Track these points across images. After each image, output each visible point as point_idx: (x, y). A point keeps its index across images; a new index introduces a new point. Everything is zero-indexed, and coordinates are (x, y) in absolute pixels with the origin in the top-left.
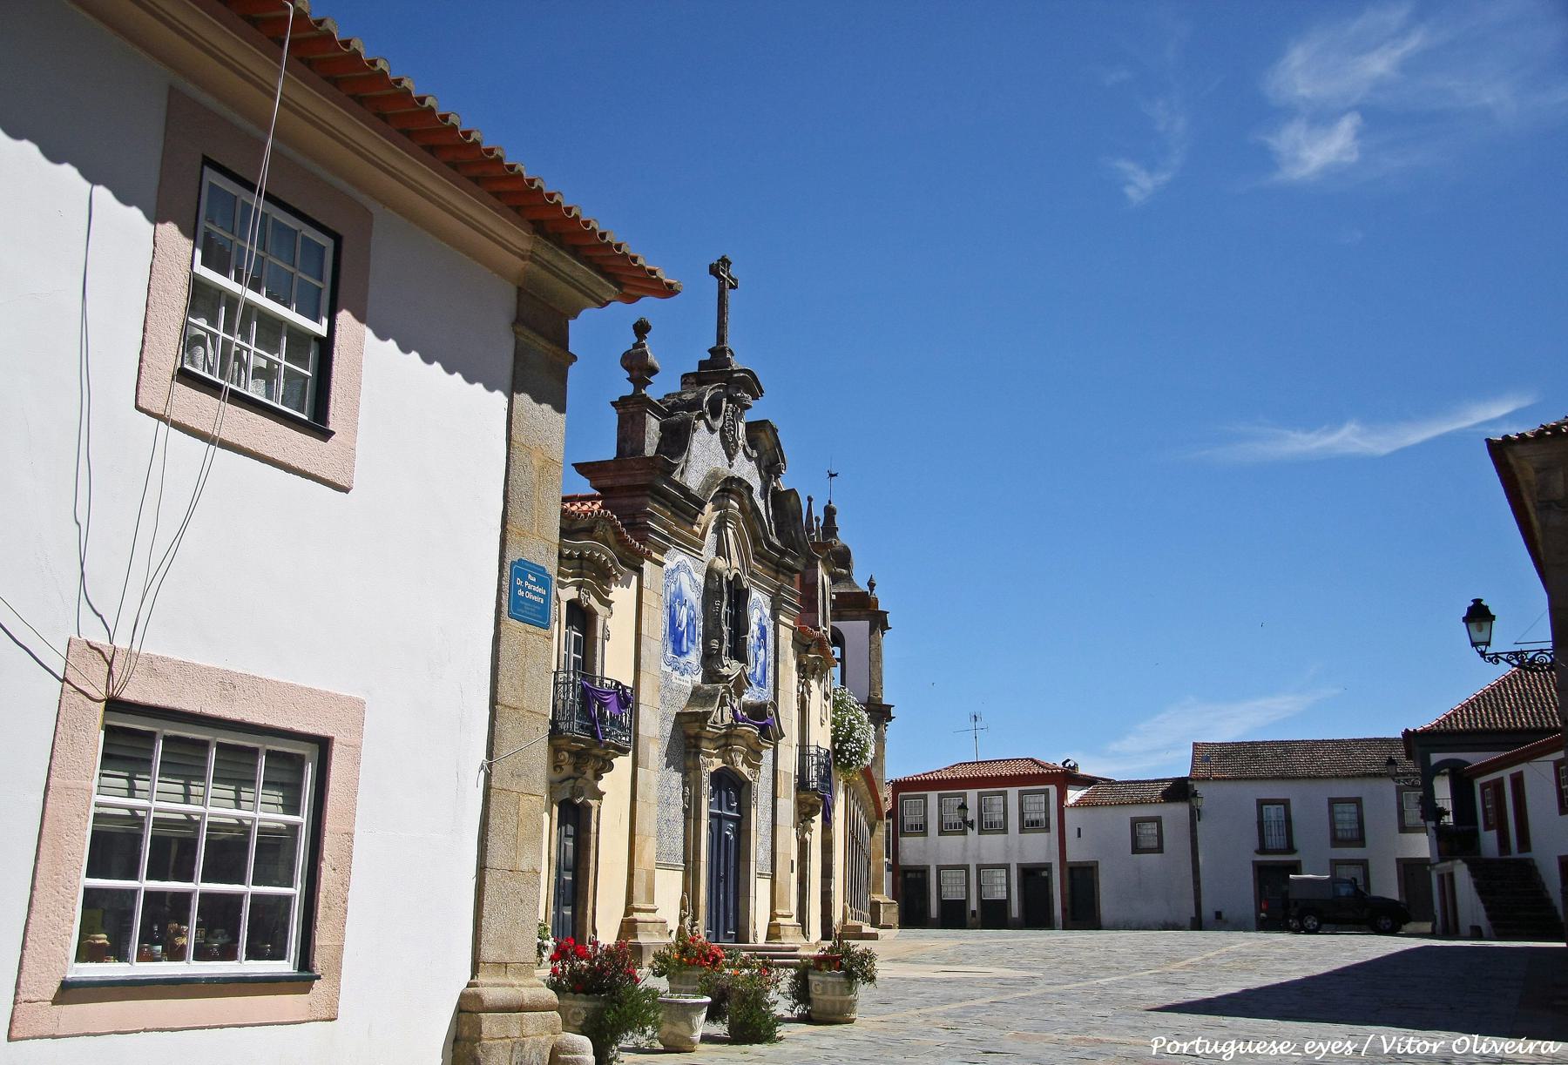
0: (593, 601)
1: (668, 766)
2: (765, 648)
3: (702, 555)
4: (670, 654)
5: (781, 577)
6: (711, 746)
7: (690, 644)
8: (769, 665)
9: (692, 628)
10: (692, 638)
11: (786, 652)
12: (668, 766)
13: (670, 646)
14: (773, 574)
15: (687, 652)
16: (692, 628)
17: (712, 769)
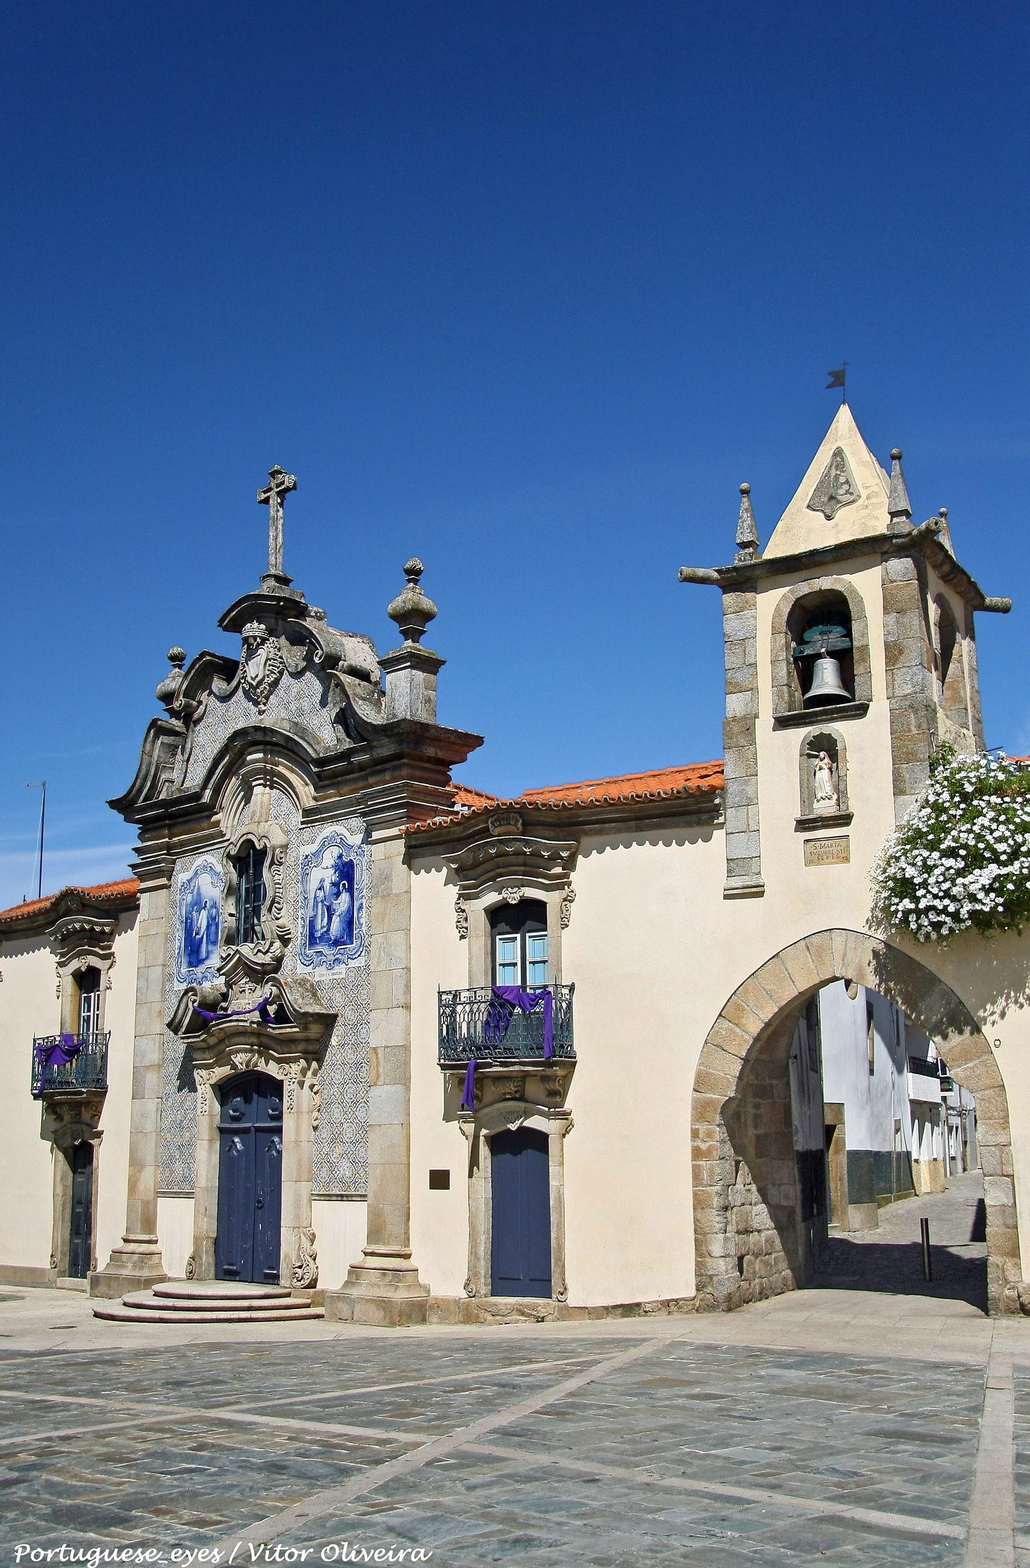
0: (94, 961)
1: (180, 1089)
2: (350, 890)
3: (228, 840)
4: (184, 970)
5: (371, 780)
6: (207, 1056)
7: (210, 948)
8: (360, 908)
9: (213, 928)
10: (212, 938)
11: (388, 878)
12: (180, 1089)
13: (185, 961)
14: (366, 783)
15: (207, 958)
16: (213, 928)
17: (212, 1082)
